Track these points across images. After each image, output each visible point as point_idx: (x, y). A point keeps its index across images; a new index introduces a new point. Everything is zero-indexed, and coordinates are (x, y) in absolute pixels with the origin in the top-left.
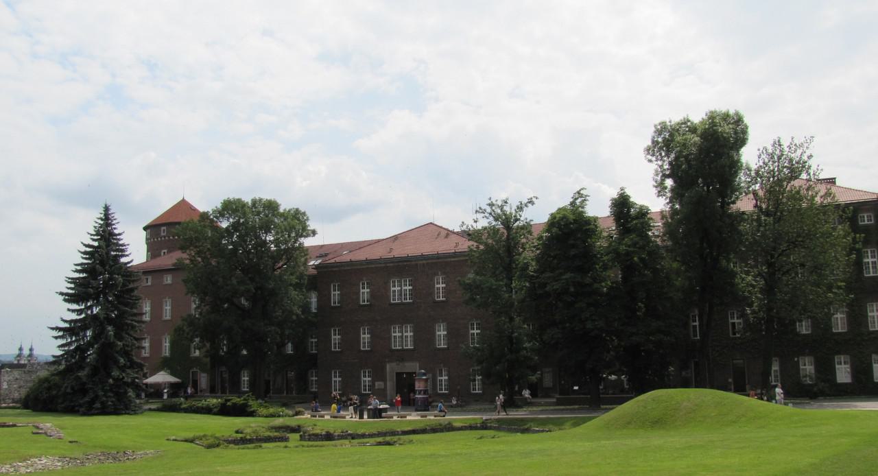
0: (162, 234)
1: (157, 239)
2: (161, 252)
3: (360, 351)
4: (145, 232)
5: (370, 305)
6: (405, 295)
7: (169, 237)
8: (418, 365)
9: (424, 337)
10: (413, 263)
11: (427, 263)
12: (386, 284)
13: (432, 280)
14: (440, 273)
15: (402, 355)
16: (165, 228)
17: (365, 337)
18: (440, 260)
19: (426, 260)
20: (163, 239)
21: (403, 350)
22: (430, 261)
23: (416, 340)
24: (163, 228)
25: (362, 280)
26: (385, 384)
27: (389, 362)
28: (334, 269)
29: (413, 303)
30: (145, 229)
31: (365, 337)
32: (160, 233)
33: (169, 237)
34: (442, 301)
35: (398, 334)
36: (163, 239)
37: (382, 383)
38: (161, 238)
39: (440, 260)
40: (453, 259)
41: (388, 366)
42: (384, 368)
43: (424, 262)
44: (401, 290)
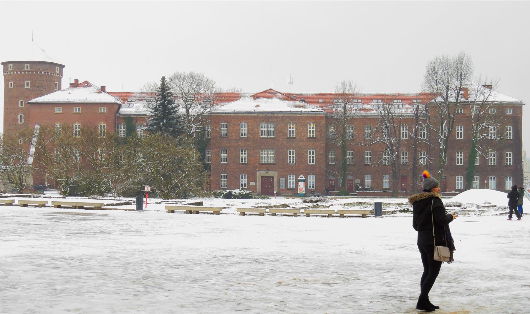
0: (26, 69)
1: (21, 72)
2: (25, 82)
3: (240, 164)
4: (3, 66)
5: (247, 138)
6: (269, 133)
7: (32, 72)
8: (277, 172)
9: (281, 158)
10: (275, 115)
11: (284, 116)
12: (258, 125)
13: (287, 126)
14: (292, 122)
15: (267, 167)
16: (28, 65)
17: (244, 156)
18: (292, 115)
19: (283, 114)
20: (27, 73)
21: (267, 164)
22: (286, 115)
23: (276, 158)
24: (26, 65)
25: (243, 123)
26: (256, 183)
27: (259, 170)
28: (223, 115)
29: (275, 138)
30: (3, 64)
31: (244, 156)
32: (24, 69)
33: (32, 72)
34: (293, 138)
35: (264, 155)
36: (27, 73)
37: (254, 183)
38: (25, 72)
39: (292, 115)
40: (300, 115)
41: (258, 173)
42: (255, 174)
43: (282, 115)
44: (267, 129)
